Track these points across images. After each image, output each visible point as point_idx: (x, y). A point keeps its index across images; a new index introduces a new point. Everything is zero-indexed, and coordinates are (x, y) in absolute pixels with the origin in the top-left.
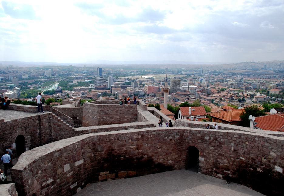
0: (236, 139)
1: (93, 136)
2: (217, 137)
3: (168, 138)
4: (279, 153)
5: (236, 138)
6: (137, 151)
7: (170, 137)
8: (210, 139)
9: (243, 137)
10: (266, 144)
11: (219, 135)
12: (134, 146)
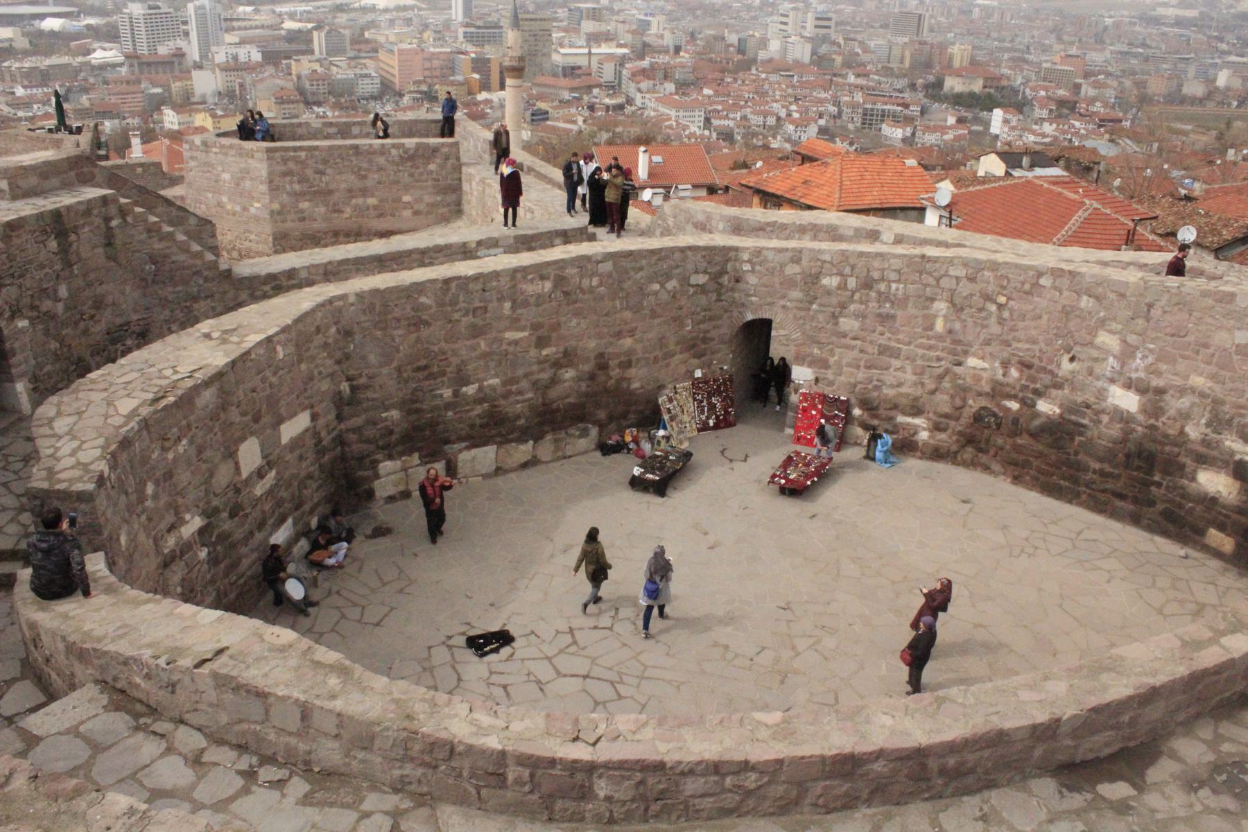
0: (958, 284)
1: (343, 297)
2: (876, 275)
3: (662, 286)
4: (1134, 337)
5: (957, 278)
6: (533, 352)
7: (672, 285)
8: (843, 286)
9: (987, 273)
10: (1085, 302)
11: (883, 270)
12: (522, 329)
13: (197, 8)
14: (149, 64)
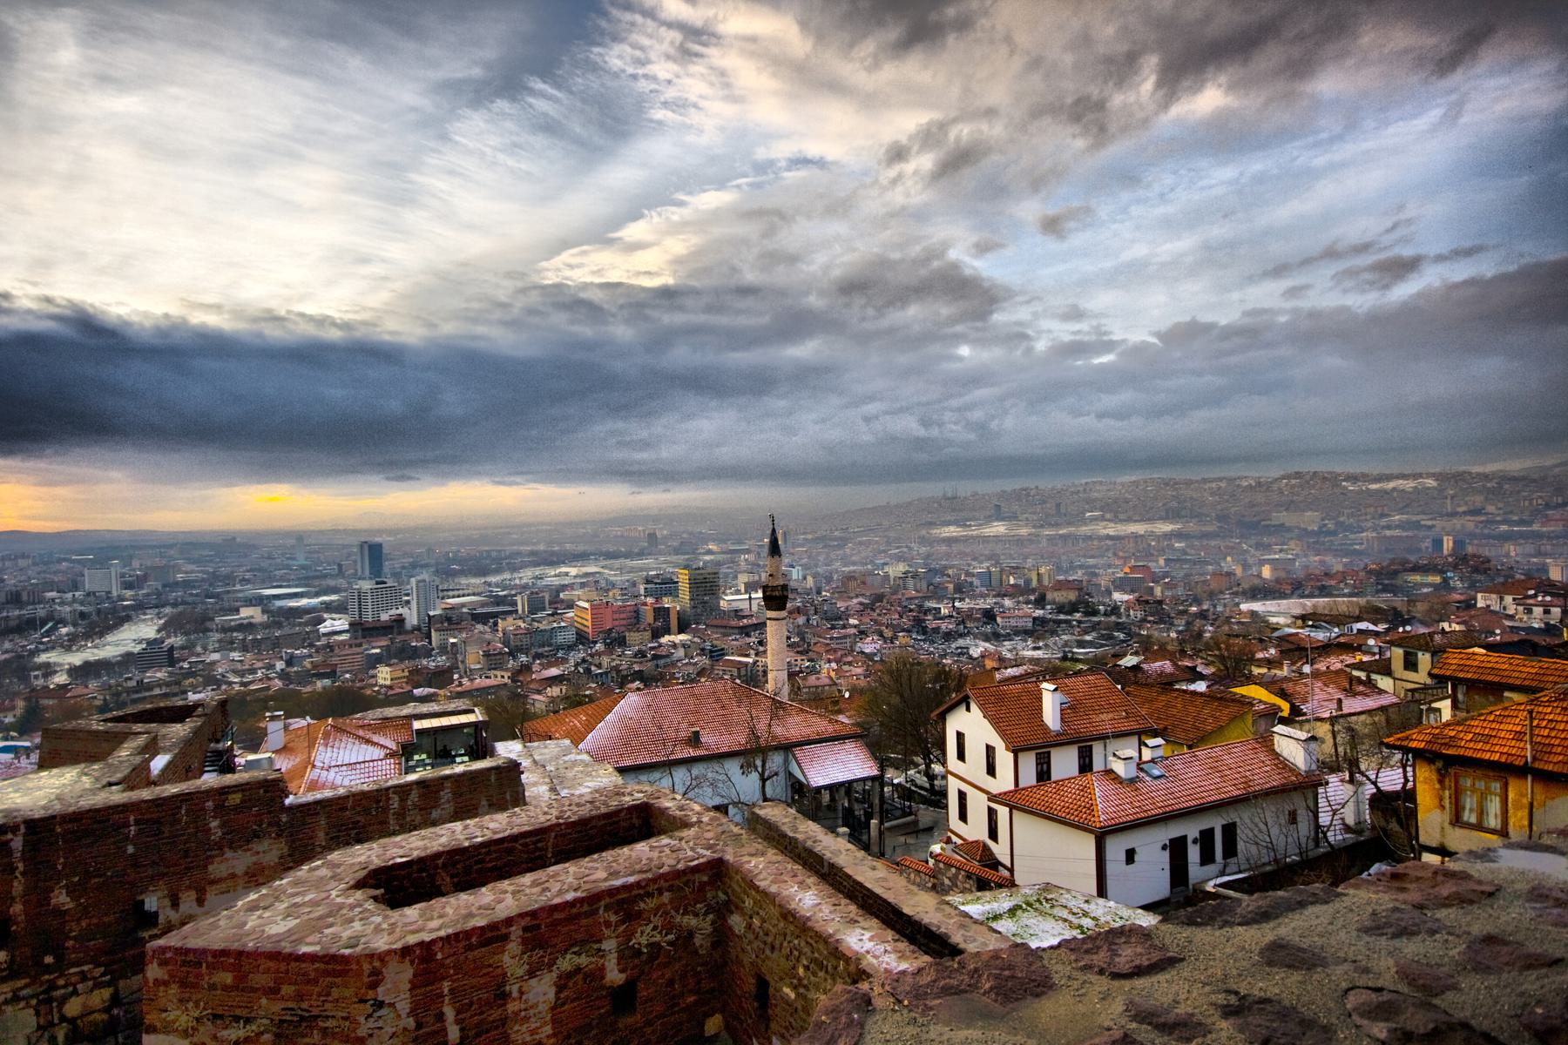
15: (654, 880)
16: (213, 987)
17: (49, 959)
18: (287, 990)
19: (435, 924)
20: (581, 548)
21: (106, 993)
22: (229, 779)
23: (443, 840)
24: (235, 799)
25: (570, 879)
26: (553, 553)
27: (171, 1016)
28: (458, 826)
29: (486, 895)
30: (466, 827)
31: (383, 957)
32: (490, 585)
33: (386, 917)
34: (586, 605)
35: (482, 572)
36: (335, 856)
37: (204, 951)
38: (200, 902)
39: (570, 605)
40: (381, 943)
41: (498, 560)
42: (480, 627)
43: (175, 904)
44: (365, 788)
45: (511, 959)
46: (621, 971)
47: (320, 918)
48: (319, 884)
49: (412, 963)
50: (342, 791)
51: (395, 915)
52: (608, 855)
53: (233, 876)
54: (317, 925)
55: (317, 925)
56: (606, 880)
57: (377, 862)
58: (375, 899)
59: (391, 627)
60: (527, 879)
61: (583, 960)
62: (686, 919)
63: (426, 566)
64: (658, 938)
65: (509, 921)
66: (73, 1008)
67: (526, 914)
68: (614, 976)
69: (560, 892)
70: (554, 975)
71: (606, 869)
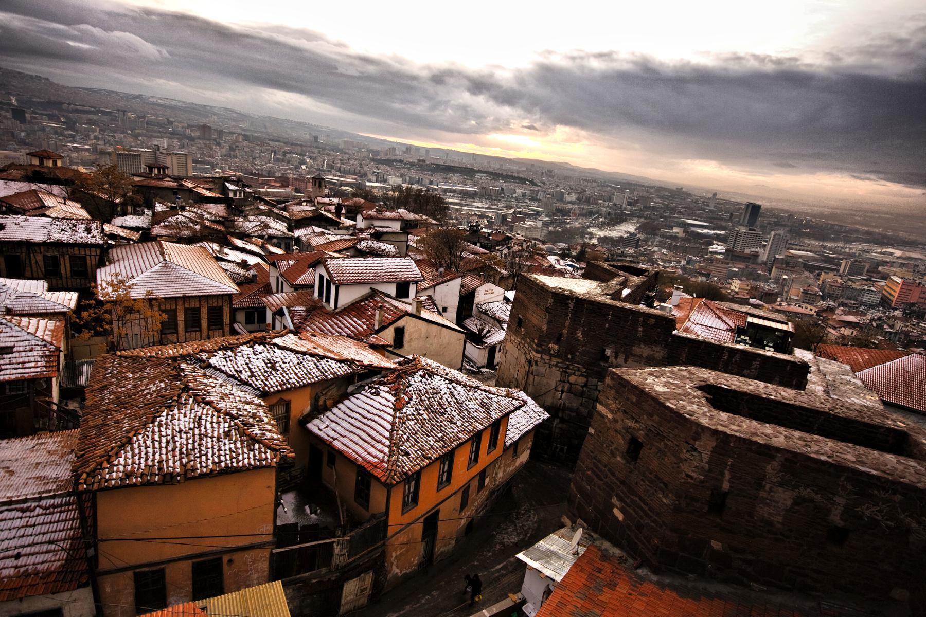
13: (775, 235)
14: (738, 256)
15: (893, 483)
16: (628, 399)
17: (570, 356)
18: (656, 418)
19: (734, 427)
20: (913, 237)
21: (584, 380)
22: (652, 311)
23: (751, 388)
24: (652, 321)
25: (827, 449)
26: (885, 237)
27: (610, 402)
28: (762, 384)
29: (768, 429)
30: (766, 387)
31: (705, 429)
32: (825, 247)
33: (710, 411)
34: (899, 281)
35: (823, 238)
36: (692, 368)
37: (628, 382)
38: (626, 361)
39: (885, 277)
40: (705, 421)
41: (837, 233)
42: (807, 274)
43: (616, 358)
44: (713, 341)
45: (771, 469)
46: (841, 519)
47: (679, 394)
48: (682, 378)
49: (717, 439)
50: (700, 338)
51: (715, 412)
52: (862, 450)
53: (641, 356)
54: (677, 397)
55: (677, 397)
56: (853, 462)
57: (712, 381)
58: (707, 399)
59: (749, 258)
60: (797, 434)
61: (818, 498)
62: (908, 520)
63: (784, 226)
64: (879, 518)
65: (778, 450)
66: (572, 379)
67: (791, 452)
68: (836, 517)
69: (817, 452)
70: (795, 494)
71: (856, 456)
